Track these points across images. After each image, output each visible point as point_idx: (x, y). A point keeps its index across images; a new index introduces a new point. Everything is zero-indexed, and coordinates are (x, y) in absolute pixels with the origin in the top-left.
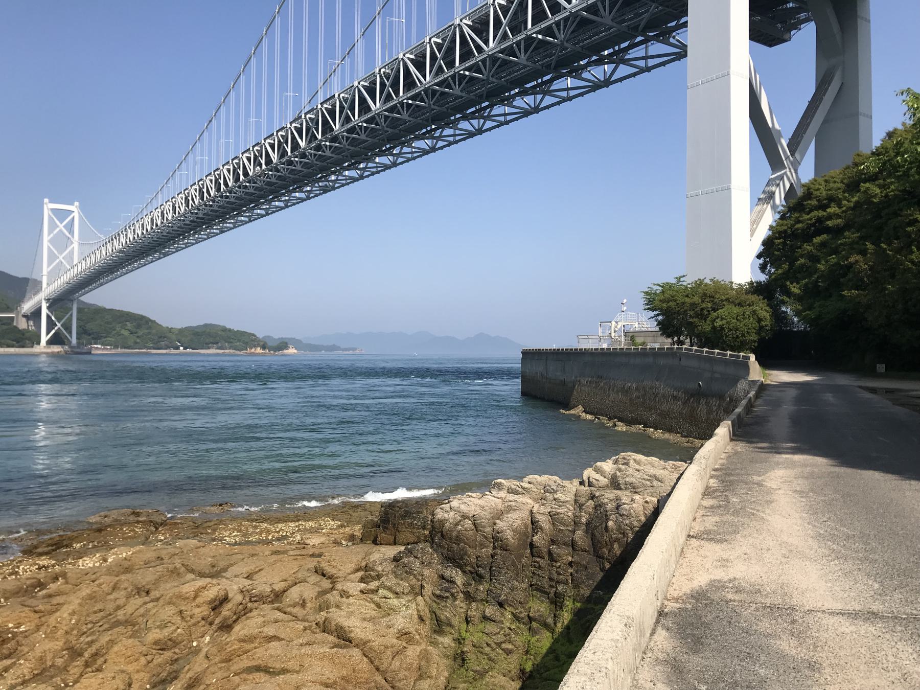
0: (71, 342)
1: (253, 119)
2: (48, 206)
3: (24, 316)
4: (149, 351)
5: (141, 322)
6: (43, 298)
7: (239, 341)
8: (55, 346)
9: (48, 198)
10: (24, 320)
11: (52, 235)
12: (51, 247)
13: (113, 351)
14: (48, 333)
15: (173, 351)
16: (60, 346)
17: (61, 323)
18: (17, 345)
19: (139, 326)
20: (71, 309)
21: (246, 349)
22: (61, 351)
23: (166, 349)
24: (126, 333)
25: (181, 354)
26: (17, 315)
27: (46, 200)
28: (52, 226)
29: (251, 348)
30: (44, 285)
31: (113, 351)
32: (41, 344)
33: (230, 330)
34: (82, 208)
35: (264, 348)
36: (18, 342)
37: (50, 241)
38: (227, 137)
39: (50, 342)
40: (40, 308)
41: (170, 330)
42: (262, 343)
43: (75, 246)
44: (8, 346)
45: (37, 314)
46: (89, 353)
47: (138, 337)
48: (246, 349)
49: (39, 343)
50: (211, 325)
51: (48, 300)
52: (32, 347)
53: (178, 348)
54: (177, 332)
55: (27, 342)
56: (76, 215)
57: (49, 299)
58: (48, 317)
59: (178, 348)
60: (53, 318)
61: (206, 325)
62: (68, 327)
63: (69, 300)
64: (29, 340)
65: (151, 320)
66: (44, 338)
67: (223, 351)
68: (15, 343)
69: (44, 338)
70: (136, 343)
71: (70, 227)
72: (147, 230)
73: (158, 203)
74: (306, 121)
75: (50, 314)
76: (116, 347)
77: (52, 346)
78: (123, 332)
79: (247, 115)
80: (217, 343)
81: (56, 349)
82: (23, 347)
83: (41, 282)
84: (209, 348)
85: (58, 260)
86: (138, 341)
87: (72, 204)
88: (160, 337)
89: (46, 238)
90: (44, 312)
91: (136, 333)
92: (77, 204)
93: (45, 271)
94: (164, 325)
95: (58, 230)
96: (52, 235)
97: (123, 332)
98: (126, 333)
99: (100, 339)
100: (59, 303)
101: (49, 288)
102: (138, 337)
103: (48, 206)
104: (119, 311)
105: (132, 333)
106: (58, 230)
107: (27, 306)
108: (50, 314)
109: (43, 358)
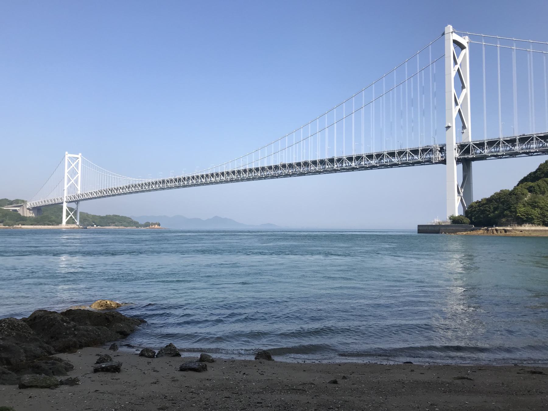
3: (28, 209)
6: (65, 200)
9: (82, 153)
10: (28, 211)
12: (69, 176)
17: (73, 212)
22: (75, 227)
26: (23, 208)
32: (63, 224)
39: (68, 223)
44: (49, 225)
51: (66, 202)
55: (54, 223)
64: (54, 222)
66: (65, 220)
68: (50, 223)
71: (77, 166)
77: (69, 225)
82: (53, 225)
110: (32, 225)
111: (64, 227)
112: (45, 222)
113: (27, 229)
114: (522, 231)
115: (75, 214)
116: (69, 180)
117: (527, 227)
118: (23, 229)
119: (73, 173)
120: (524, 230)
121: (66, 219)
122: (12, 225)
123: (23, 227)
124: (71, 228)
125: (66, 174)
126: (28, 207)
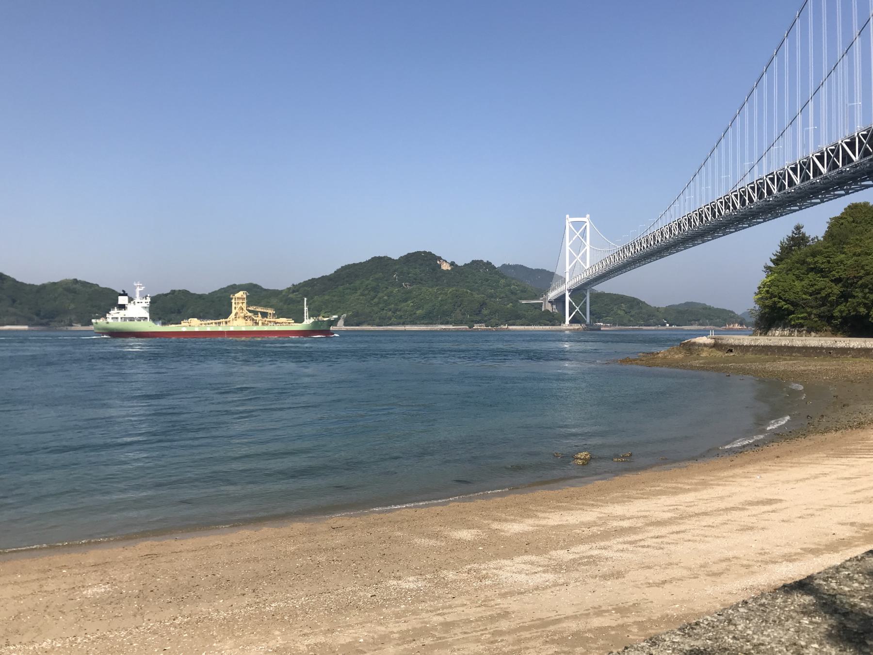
0: (586, 321)
1: (723, 177)
2: (569, 220)
3: (549, 302)
4: (641, 327)
5: (633, 303)
6: (568, 286)
7: (719, 317)
8: (575, 325)
11: (572, 241)
13: (612, 328)
14: (570, 316)
15: (660, 328)
16: (579, 325)
18: (550, 324)
19: (632, 307)
20: (586, 296)
21: (725, 325)
23: (655, 326)
24: (621, 313)
25: (667, 330)
26: (545, 302)
27: (567, 216)
28: (572, 234)
29: (729, 325)
30: (567, 280)
31: (612, 328)
32: (566, 323)
33: (710, 308)
34: (591, 218)
35: (741, 324)
36: (550, 322)
37: (570, 246)
38: (707, 185)
40: (564, 295)
41: (658, 309)
42: (739, 320)
43: (588, 248)
44: (545, 325)
45: (560, 300)
46: (600, 330)
47: (631, 316)
48: (725, 325)
49: (564, 322)
50: (692, 303)
51: (569, 290)
52: (560, 325)
53: (664, 325)
54: (663, 311)
56: (588, 224)
57: (571, 289)
58: (570, 303)
59: (664, 325)
60: (574, 304)
61: (687, 304)
62: (583, 309)
63: (584, 289)
65: (641, 301)
66: (568, 319)
67: (704, 327)
69: (568, 319)
70: (630, 321)
72: (651, 245)
73: (658, 226)
74: (757, 185)
75: (572, 301)
76: (614, 325)
78: (619, 312)
79: (720, 175)
80: (698, 320)
81: (576, 326)
83: (565, 279)
84: (692, 325)
85: (576, 260)
86: (632, 319)
87: (585, 217)
88: (649, 316)
89: (568, 243)
90: (568, 299)
91: (629, 313)
92: (588, 216)
93: (568, 268)
94: (653, 305)
95: (576, 236)
96: (572, 241)
97: (619, 312)
98: (621, 313)
99: (602, 318)
100: (577, 292)
101: (570, 282)
102: (631, 316)
103: (569, 220)
104: (615, 294)
105: (626, 313)
106: (576, 236)
107: (552, 295)
108: (572, 301)
109: (567, 332)
110: (522, 325)
111: (565, 328)
112: (541, 321)
113: (514, 331)
114: (731, 351)
115: (583, 309)
116: (572, 258)
117: (778, 338)
118: (510, 330)
119: (578, 246)
120: (736, 347)
121: (570, 316)
122: (497, 325)
123: (510, 327)
124: (574, 329)
125: (568, 248)
126: (549, 298)
